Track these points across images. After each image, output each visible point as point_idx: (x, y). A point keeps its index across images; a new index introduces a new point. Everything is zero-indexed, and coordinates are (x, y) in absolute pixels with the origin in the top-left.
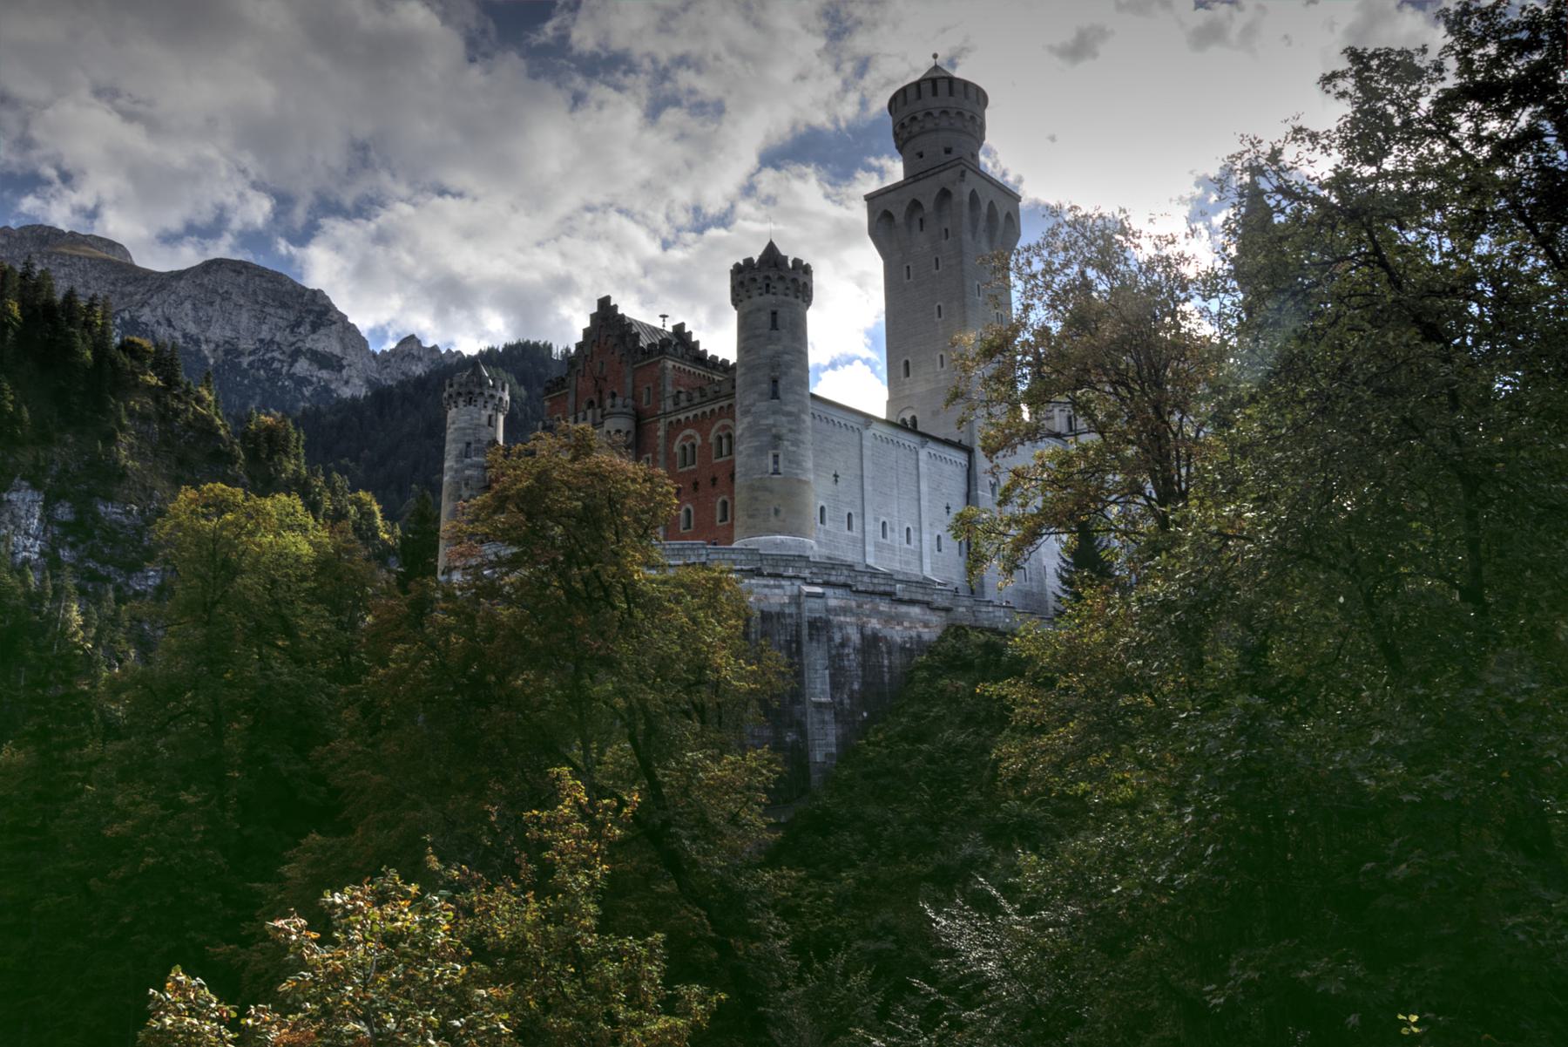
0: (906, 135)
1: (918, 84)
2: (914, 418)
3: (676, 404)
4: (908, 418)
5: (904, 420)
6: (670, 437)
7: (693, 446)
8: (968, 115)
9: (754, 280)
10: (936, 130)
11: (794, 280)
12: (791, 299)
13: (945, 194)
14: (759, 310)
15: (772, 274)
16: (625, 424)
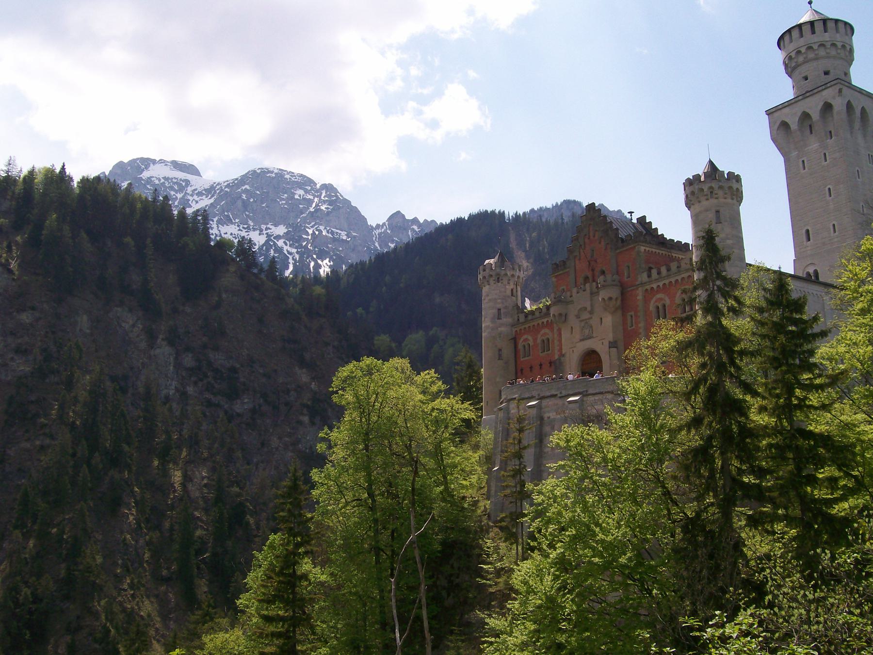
0: (793, 65)
1: (800, 26)
2: (816, 272)
3: (649, 276)
4: (811, 271)
5: (808, 274)
6: (646, 300)
7: (664, 306)
8: (839, 45)
9: (702, 190)
10: (817, 59)
11: (730, 188)
12: (729, 201)
13: (827, 107)
14: (707, 210)
15: (714, 185)
16: (615, 293)
